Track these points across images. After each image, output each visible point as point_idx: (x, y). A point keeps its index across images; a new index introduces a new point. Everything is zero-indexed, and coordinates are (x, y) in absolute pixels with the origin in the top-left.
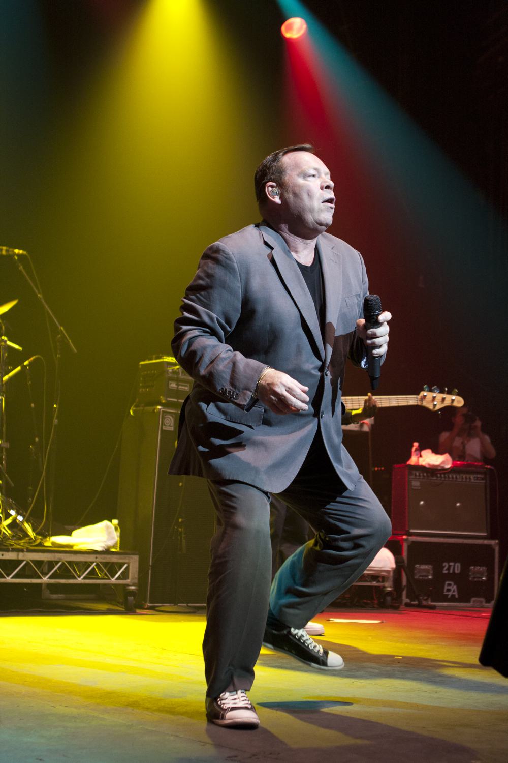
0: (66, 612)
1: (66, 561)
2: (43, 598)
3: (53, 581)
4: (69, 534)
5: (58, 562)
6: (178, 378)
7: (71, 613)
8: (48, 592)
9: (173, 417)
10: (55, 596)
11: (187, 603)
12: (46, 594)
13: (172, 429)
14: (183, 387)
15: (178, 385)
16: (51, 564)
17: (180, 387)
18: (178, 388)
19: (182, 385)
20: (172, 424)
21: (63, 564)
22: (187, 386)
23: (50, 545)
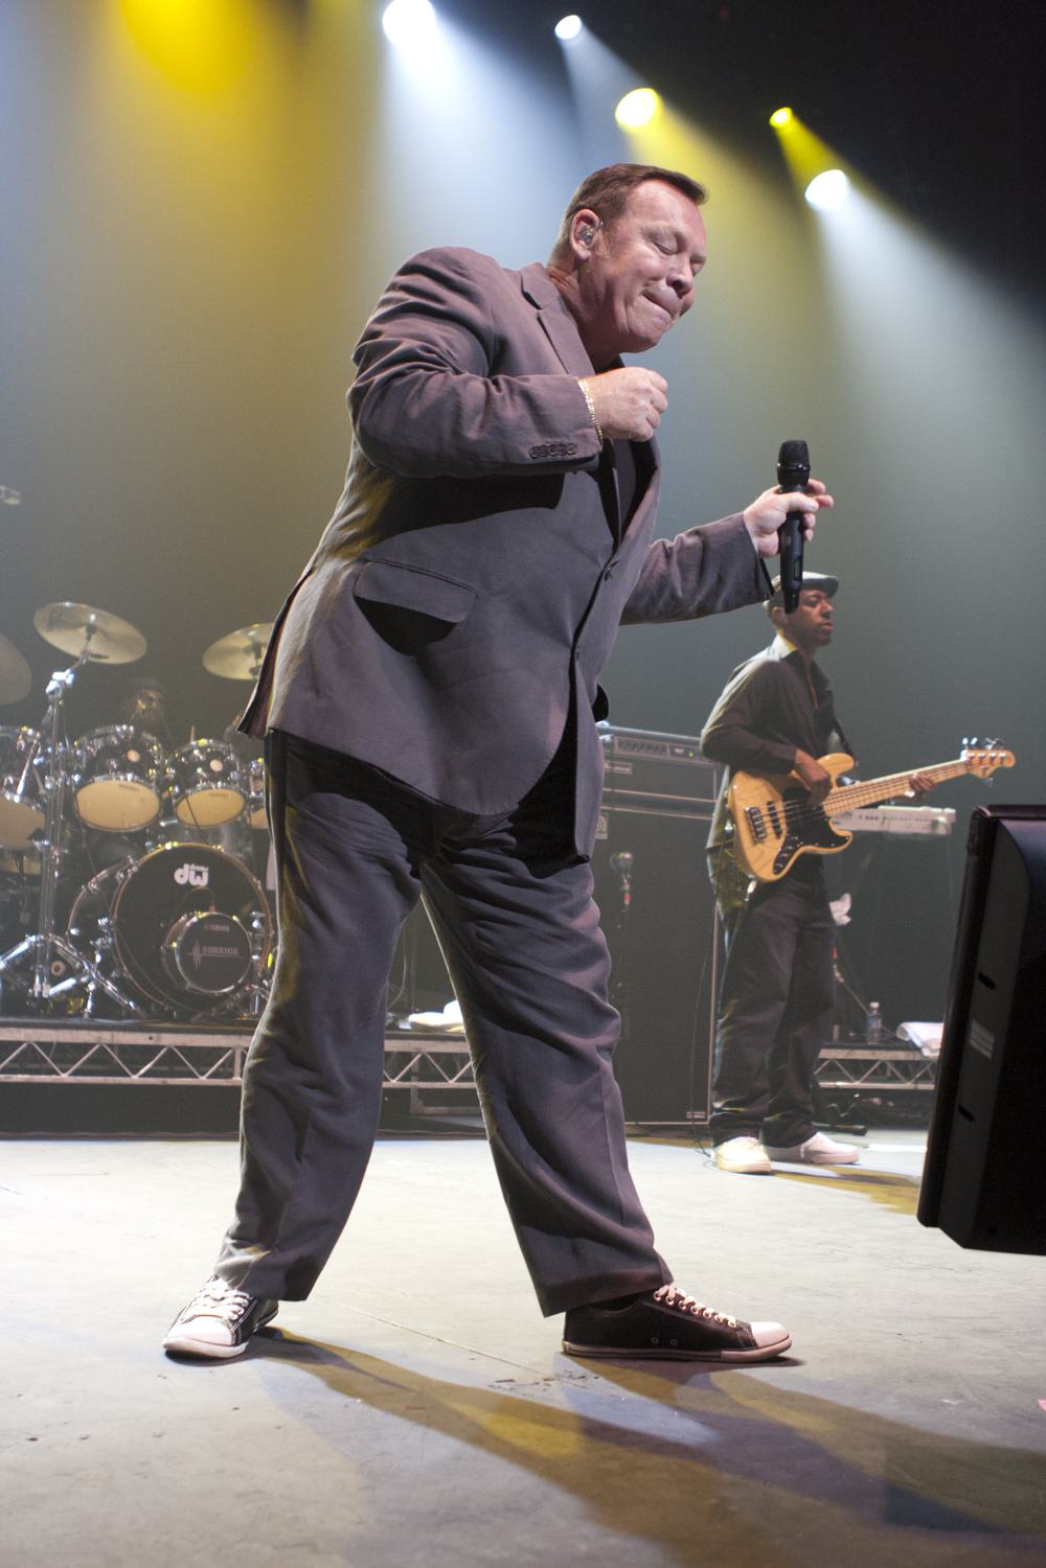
0: (427, 1134)
1: (431, 1054)
2: (412, 1111)
3: (406, 1085)
4: (441, 1010)
5: (417, 1053)
6: (611, 753)
7: (409, 1134)
8: (421, 1103)
9: (605, 816)
10: (431, 1110)
11: (637, 1120)
12: (416, 1104)
13: (604, 837)
14: (621, 769)
15: (612, 765)
16: (406, 1057)
17: (616, 768)
18: (612, 769)
19: (620, 766)
20: (605, 830)
21: (423, 1059)
22: (627, 766)
23: (408, 1027)
